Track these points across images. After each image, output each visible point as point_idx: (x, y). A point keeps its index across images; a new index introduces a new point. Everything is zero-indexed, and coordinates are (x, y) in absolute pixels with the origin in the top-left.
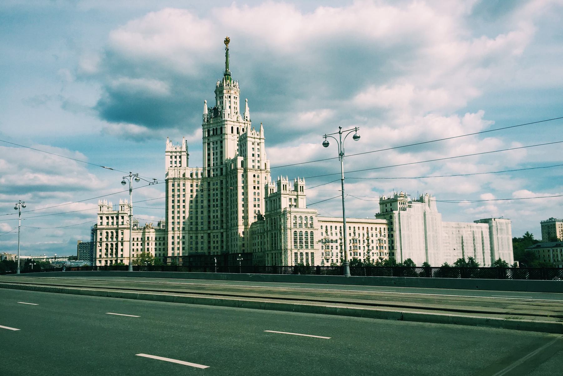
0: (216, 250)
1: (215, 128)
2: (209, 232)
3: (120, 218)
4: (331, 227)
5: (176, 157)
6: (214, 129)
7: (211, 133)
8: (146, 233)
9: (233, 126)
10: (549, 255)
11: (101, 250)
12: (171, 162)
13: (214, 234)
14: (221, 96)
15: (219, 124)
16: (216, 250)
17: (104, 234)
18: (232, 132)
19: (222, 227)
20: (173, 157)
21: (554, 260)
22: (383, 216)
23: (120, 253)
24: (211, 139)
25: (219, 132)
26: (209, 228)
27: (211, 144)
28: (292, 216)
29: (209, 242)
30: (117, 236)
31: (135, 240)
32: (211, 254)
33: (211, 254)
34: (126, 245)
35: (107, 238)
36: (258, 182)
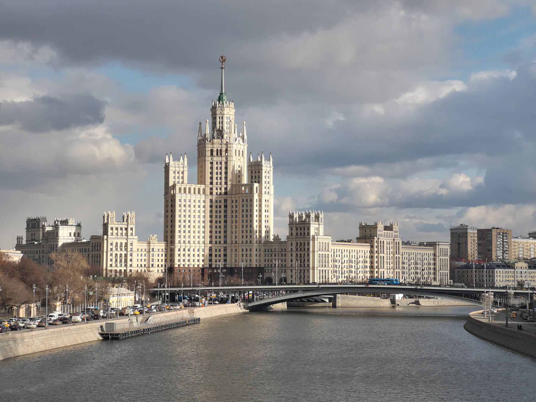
1: (219, 150)
3: (129, 229)
4: (337, 250)
5: (178, 173)
6: (217, 150)
7: (215, 153)
8: (151, 245)
9: (236, 149)
10: (472, 275)
11: (111, 260)
16: (218, 263)
17: (114, 245)
18: (236, 155)
19: (225, 242)
21: (480, 280)
22: (364, 240)
23: (129, 263)
24: (215, 159)
27: (215, 163)
28: (318, 242)
31: (140, 250)
32: (213, 267)
33: (213, 267)
34: (134, 254)
35: (117, 250)
36: (268, 205)
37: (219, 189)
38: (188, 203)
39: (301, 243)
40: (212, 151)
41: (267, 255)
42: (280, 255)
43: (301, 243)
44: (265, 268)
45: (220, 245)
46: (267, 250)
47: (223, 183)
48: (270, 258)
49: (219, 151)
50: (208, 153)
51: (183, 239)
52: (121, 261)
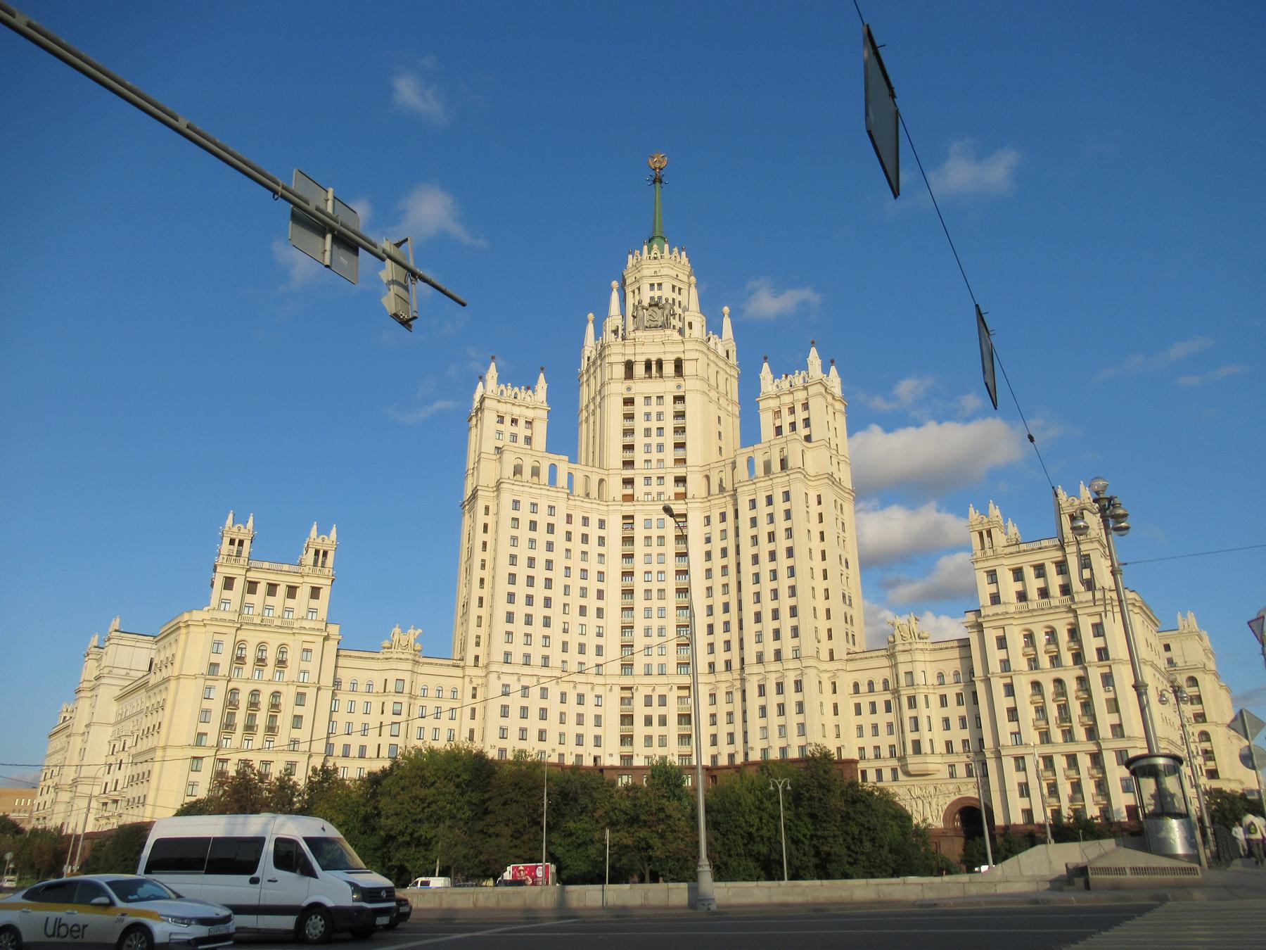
0: (657, 752)
2: (627, 681)
5: (514, 421)
7: (639, 370)
12: (499, 433)
13: (648, 691)
14: (656, 281)
15: (668, 348)
20: (508, 420)
24: (642, 387)
25: (669, 369)
26: (627, 667)
27: (639, 401)
29: (627, 719)
30: (281, 663)
37: (654, 480)
38: (542, 519)
39: (1052, 634)
40: (629, 366)
41: (866, 709)
42: (935, 701)
43: (1052, 634)
44: (861, 766)
45: (663, 680)
46: (864, 688)
47: (670, 462)
48: (882, 718)
49: (654, 363)
50: (620, 371)
51: (518, 650)
52: (250, 728)
